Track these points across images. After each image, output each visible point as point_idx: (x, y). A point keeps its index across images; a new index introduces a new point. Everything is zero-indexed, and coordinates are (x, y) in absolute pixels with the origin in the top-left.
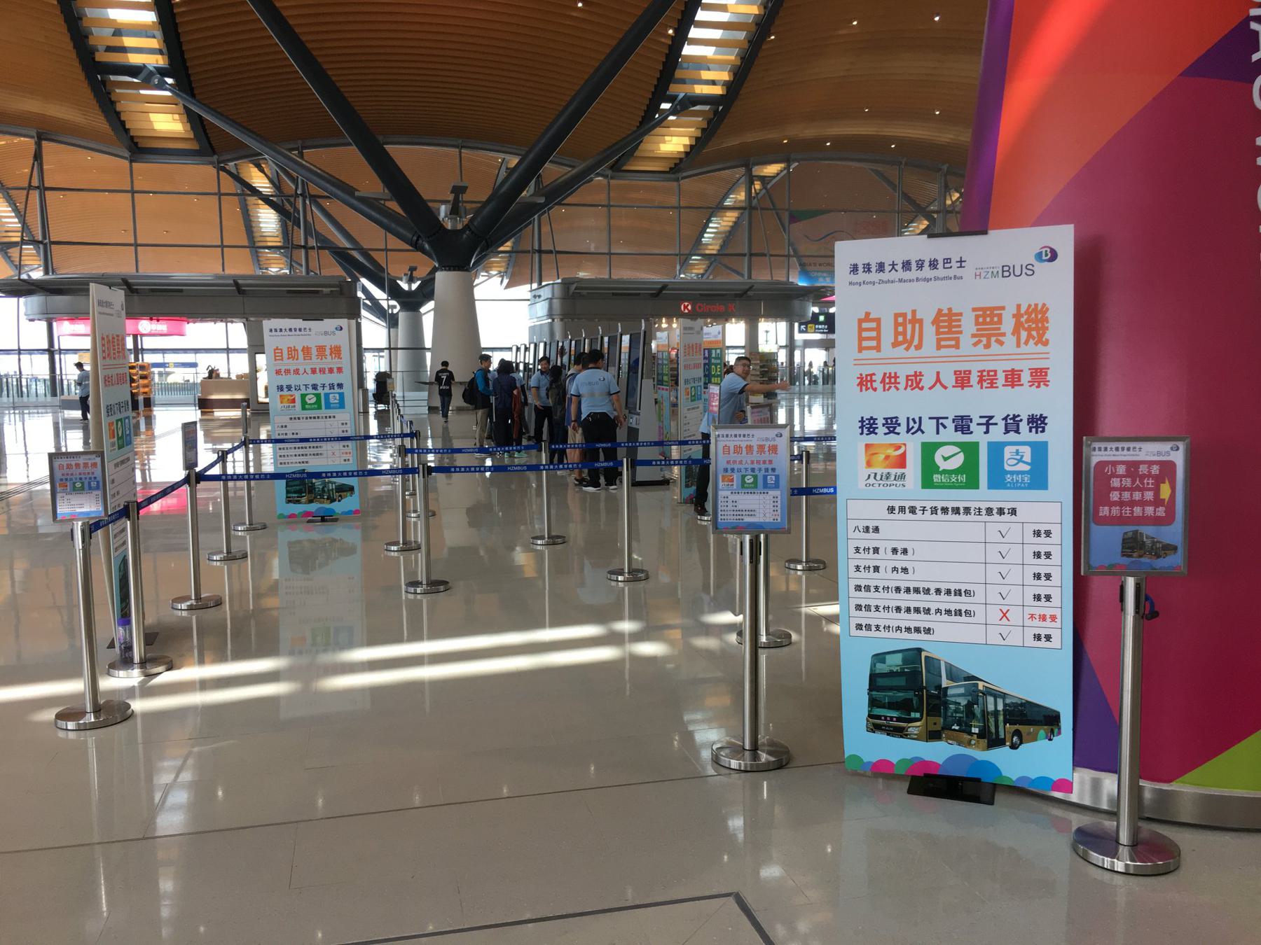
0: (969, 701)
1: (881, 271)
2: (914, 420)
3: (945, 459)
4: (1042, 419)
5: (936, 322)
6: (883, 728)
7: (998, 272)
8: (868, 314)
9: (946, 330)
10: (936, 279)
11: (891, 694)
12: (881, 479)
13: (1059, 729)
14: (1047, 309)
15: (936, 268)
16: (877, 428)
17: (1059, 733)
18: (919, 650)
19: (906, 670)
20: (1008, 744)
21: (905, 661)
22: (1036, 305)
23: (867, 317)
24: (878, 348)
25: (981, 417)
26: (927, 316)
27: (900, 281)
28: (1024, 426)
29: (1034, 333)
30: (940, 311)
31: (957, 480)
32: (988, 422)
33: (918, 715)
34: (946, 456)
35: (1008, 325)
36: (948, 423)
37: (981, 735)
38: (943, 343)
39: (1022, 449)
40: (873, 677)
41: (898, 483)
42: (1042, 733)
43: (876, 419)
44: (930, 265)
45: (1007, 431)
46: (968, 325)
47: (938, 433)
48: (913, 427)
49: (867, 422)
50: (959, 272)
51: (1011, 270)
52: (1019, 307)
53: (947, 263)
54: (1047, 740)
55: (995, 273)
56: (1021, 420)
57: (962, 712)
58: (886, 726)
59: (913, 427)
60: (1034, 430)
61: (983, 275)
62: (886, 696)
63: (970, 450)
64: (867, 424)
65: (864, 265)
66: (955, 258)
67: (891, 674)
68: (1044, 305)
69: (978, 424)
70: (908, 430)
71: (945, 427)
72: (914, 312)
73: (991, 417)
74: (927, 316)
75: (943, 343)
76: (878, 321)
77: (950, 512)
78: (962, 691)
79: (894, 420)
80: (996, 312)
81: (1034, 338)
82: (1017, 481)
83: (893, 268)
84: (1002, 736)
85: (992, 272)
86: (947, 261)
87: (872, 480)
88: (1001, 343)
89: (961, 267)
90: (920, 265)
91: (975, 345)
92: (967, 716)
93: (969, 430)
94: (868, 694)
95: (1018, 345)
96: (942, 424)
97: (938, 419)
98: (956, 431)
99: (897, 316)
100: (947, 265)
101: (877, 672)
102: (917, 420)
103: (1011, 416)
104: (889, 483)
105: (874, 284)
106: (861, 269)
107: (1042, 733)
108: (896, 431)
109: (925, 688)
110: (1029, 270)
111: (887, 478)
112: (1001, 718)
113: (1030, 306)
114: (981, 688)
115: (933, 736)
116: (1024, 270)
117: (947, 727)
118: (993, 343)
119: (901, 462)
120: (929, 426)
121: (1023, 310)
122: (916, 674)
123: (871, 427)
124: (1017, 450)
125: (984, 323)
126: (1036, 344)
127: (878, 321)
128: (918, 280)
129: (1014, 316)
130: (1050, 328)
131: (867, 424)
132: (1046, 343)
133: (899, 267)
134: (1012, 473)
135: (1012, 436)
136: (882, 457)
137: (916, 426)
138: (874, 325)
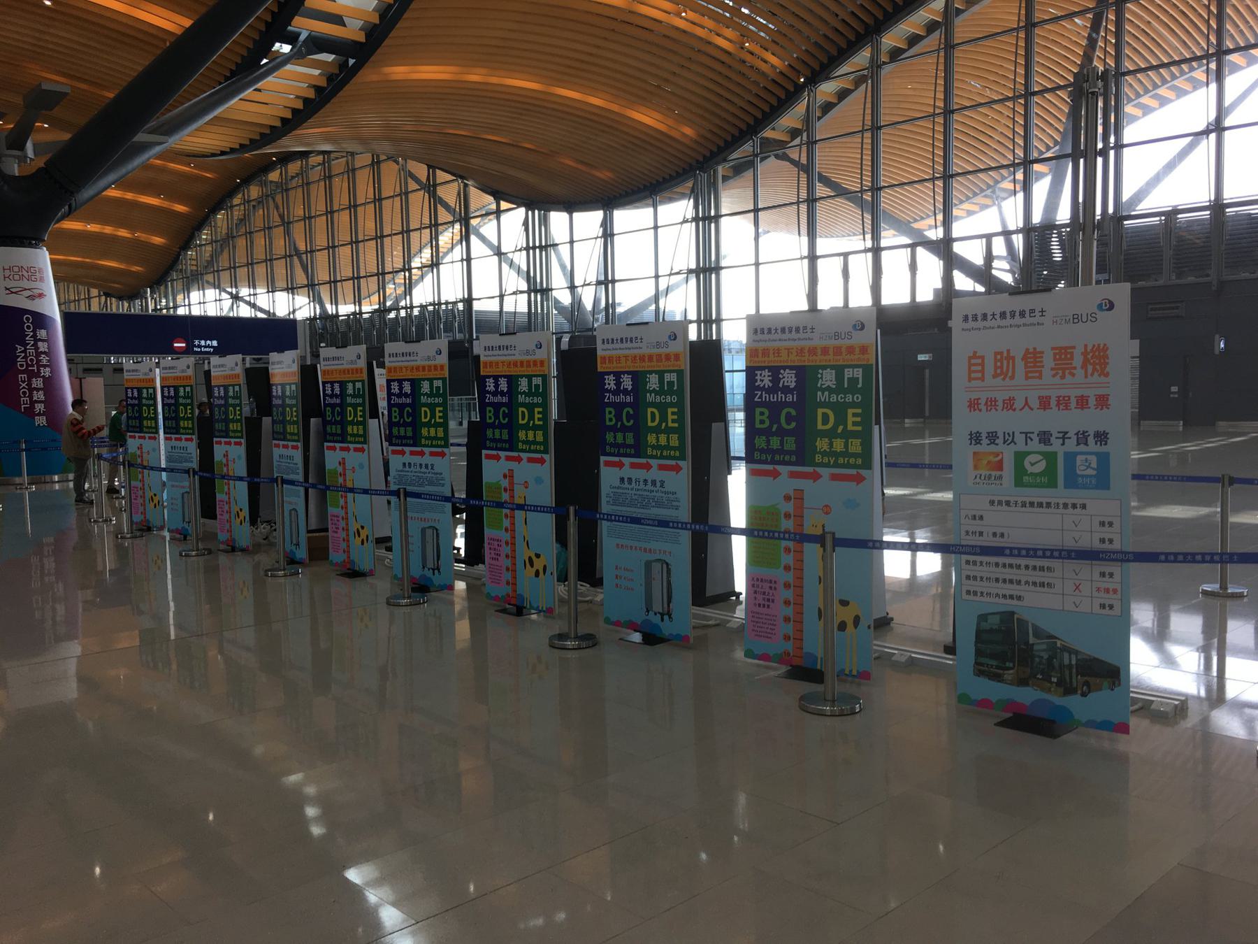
3: (1032, 465)
5: (1024, 358)
8: (975, 353)
10: (1025, 325)
14: (1107, 349)
18: (1013, 613)
22: (1099, 345)
23: (975, 356)
24: (982, 379)
25: (1059, 432)
26: (1018, 354)
27: (999, 327)
28: (1091, 440)
29: (1098, 367)
30: (1027, 349)
33: (1011, 665)
34: (1033, 462)
35: (1078, 360)
36: (1034, 436)
37: (1059, 684)
38: (1030, 375)
39: (1089, 457)
40: (979, 633)
41: (997, 482)
45: (1078, 444)
46: (1048, 361)
47: (1026, 444)
50: (1041, 320)
52: (1086, 346)
60: (1099, 443)
63: (1051, 458)
67: (991, 631)
69: (1057, 438)
71: (1032, 440)
72: (1008, 351)
73: (1066, 433)
75: (1030, 375)
76: (982, 358)
78: (1044, 647)
82: (1087, 483)
86: (1032, 311)
87: (978, 480)
88: (1073, 375)
90: (1013, 315)
91: (1054, 376)
95: (1086, 377)
96: (1030, 438)
97: (1026, 433)
99: (996, 354)
108: (996, 442)
110: (1092, 318)
111: (989, 479)
112: (1074, 671)
113: (1094, 346)
114: (1059, 645)
115: (1022, 682)
116: (1090, 318)
119: (999, 466)
120: (1020, 439)
121: (1089, 348)
125: (1060, 359)
126: (1100, 375)
127: (982, 358)
132: (1107, 375)
133: (997, 317)
134: (1083, 476)
135: (1082, 448)
136: (985, 462)
137: (1010, 439)
138: (979, 361)
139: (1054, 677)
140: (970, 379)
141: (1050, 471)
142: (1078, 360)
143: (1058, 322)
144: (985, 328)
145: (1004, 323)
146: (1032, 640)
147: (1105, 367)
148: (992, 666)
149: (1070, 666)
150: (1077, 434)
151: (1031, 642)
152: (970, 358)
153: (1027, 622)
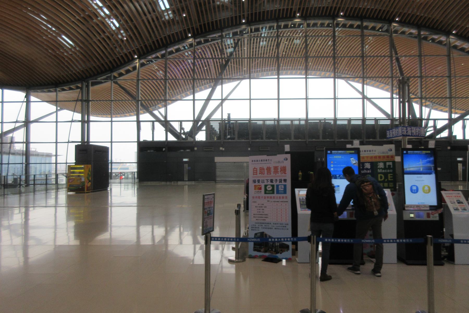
5: (267, 169)
18: (263, 233)
23: (255, 168)
24: (257, 174)
26: (265, 168)
35: (279, 170)
37: (275, 251)
46: (272, 170)
74: (265, 168)
76: (257, 169)
99: (260, 168)
115: (265, 252)
127: (257, 169)
132: (286, 174)
140: (254, 174)
142: (279, 170)
149: (277, 246)
152: (254, 169)
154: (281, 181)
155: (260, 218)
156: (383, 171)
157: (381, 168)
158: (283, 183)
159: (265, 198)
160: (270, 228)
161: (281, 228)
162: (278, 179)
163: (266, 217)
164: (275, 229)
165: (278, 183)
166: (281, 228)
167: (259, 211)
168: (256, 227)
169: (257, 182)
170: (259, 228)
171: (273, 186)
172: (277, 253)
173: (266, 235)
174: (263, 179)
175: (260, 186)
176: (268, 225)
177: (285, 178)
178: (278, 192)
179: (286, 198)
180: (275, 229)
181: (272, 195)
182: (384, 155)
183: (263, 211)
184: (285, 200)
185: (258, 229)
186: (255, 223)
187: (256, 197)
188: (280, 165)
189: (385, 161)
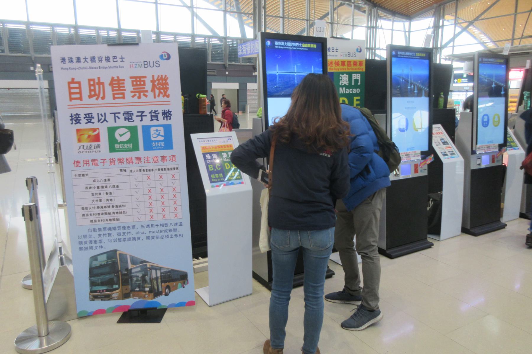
0: (143, 274)
1: (79, 62)
2: (101, 114)
3: (121, 136)
4: (169, 112)
5: (111, 84)
6: (99, 297)
7: (142, 65)
8: (73, 79)
9: (117, 89)
11: (101, 277)
12: (87, 149)
13: (188, 281)
14: (167, 78)
15: (109, 61)
16: (81, 120)
17: (188, 283)
18: (115, 251)
19: (109, 263)
20: (164, 293)
21: (108, 258)
22: (162, 76)
23: (73, 81)
24: (81, 99)
25: (138, 112)
26: (106, 81)
27: (90, 68)
28: (160, 116)
29: (162, 91)
30: (113, 78)
31: (128, 147)
32: (142, 115)
33: (117, 286)
34: (121, 134)
35: (149, 86)
36: (121, 116)
37: (150, 292)
38: (116, 96)
39: (159, 128)
40: (91, 270)
41: (97, 150)
42: (180, 285)
43: (80, 115)
44: (106, 60)
45: (152, 120)
46: (128, 86)
47: (115, 122)
48: (101, 119)
49: (75, 116)
50: (122, 64)
51: (148, 64)
52: (153, 76)
53: (115, 59)
54: (182, 288)
55: (140, 65)
56: (159, 113)
57: (140, 281)
58: (100, 296)
59: (101, 119)
60: (165, 118)
61: (134, 66)
62: (99, 279)
63: (133, 130)
64: (75, 118)
65: (69, 58)
66: (119, 56)
67: (101, 266)
68: (166, 76)
69: (137, 116)
70: (99, 121)
71: (119, 118)
72: (99, 78)
73: (143, 112)
74: (106, 81)
75: (116, 96)
76: (79, 83)
77: (125, 162)
78: (139, 269)
79: (90, 115)
80: (142, 79)
81: (162, 93)
82: (158, 146)
83: (86, 60)
84: (160, 290)
85: (139, 65)
86: (115, 57)
87: (81, 150)
88: (146, 96)
89: (122, 61)
91: (133, 97)
92: (143, 282)
93: (132, 120)
94: (89, 279)
95: (155, 97)
96: (117, 117)
97: (115, 114)
98: (125, 120)
99: (90, 80)
100: (115, 60)
101: (93, 266)
102: (103, 115)
103: (154, 111)
104: (91, 150)
105: (76, 70)
106: (67, 61)
107: (180, 285)
108: (92, 121)
109: (120, 271)
111: (90, 148)
112: (159, 281)
113: (159, 76)
114: (148, 266)
115: (126, 296)
116: (155, 64)
117: (133, 290)
118: (142, 96)
119: (97, 138)
120: (110, 118)
121: (156, 78)
122: (115, 264)
123: (77, 120)
124: (157, 129)
125: (137, 85)
126: (164, 96)
127: (79, 83)
128: (100, 67)
129: (151, 81)
130: (170, 88)
131: (75, 118)
132: (168, 96)
133: (89, 60)
134: (155, 141)
135: (155, 122)
136: (86, 136)
137: (103, 118)
138: (77, 85)
139: (147, 287)
140: (71, 99)
141: (134, 140)
142: (149, 86)
143: (134, 67)
144: (80, 68)
145: (93, 65)
146: (130, 266)
147: (167, 91)
148: (103, 291)
149: (157, 278)
150: (150, 113)
151: (130, 268)
152: (69, 83)
153: (126, 255)
154: (154, 116)
155: (101, 217)
156: (348, 91)
157: (345, 86)
158: (162, 121)
159: (112, 162)
160: (134, 239)
161: (164, 234)
162: (147, 110)
163: (121, 213)
164: (148, 238)
165: (147, 121)
166: (164, 234)
167: (98, 197)
168: (93, 239)
169: (83, 121)
170: (100, 241)
171: (133, 130)
172: (158, 294)
173: (123, 257)
174: (102, 111)
175: (95, 130)
176: (126, 231)
177: (166, 108)
178: (148, 146)
179: (173, 158)
180: (148, 238)
181: (133, 155)
182: (350, 59)
183: (109, 197)
184: (169, 164)
185: (98, 245)
186: (90, 230)
187: (86, 162)
188: (149, 73)
189: (351, 71)
